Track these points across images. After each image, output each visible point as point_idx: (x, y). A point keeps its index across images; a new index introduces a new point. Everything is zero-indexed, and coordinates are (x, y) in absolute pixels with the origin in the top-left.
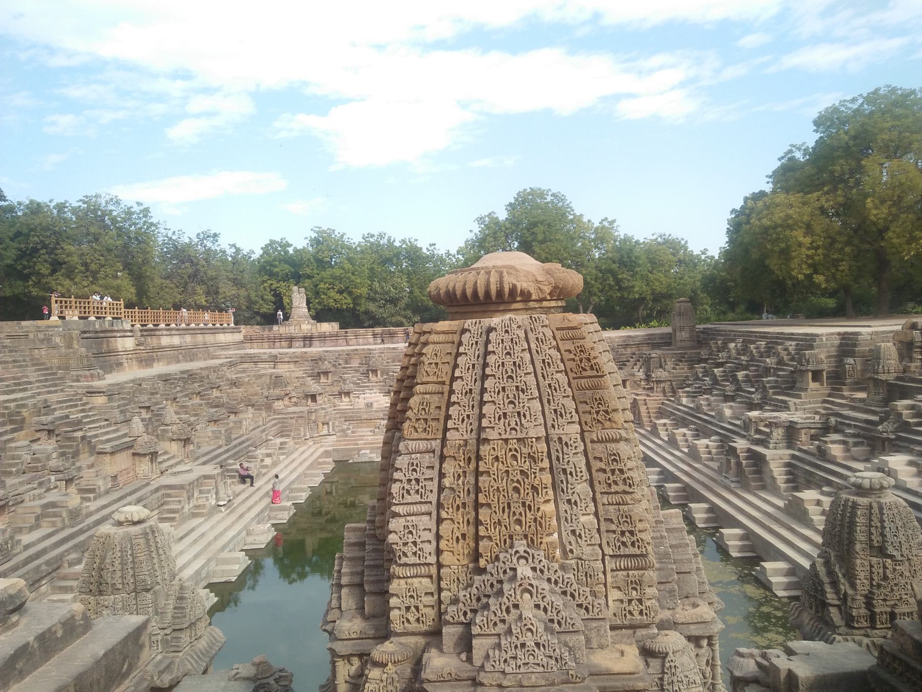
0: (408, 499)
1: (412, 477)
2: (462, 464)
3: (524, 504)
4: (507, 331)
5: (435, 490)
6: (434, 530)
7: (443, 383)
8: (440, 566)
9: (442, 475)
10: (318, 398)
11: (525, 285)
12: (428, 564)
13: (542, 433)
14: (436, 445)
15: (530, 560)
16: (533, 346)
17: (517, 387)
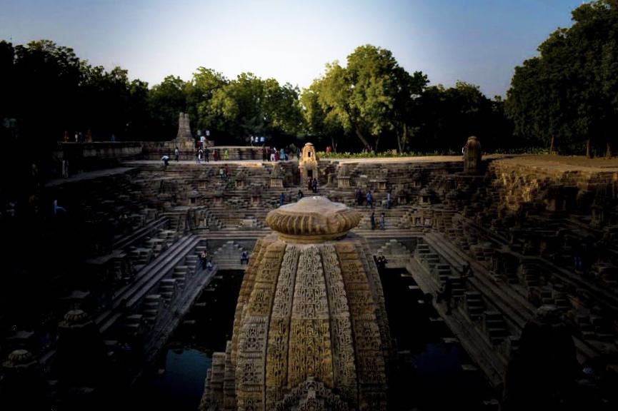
0: (250, 349)
1: (252, 337)
2: (280, 332)
3: (314, 358)
4: (310, 256)
5: (265, 345)
6: (263, 368)
7: (272, 283)
8: (266, 387)
9: (268, 338)
10: (196, 201)
11: (323, 226)
12: (259, 386)
13: (327, 317)
14: (266, 319)
15: (316, 388)
16: (325, 264)
17: (314, 290)
